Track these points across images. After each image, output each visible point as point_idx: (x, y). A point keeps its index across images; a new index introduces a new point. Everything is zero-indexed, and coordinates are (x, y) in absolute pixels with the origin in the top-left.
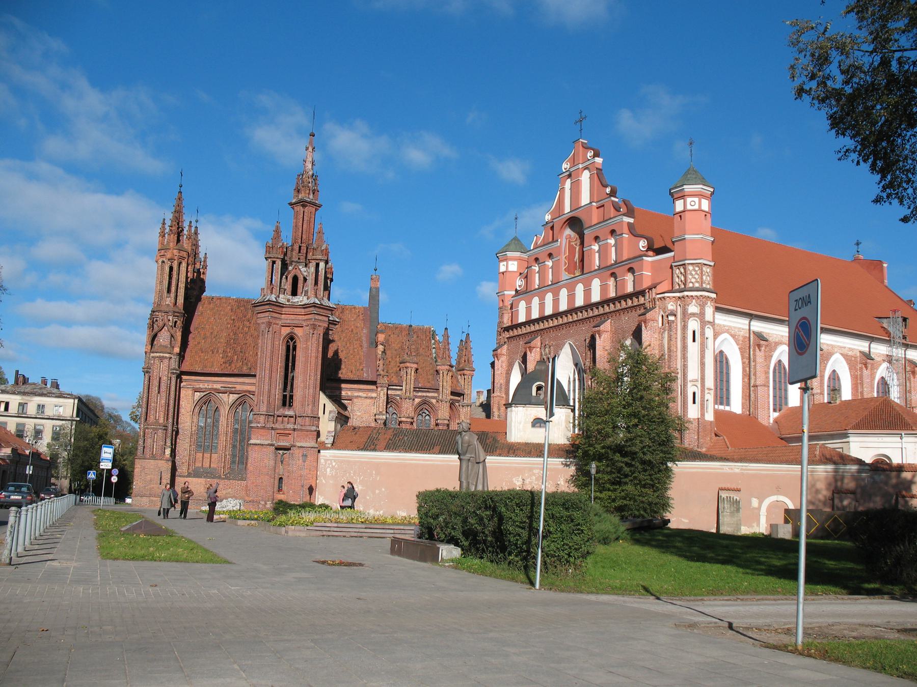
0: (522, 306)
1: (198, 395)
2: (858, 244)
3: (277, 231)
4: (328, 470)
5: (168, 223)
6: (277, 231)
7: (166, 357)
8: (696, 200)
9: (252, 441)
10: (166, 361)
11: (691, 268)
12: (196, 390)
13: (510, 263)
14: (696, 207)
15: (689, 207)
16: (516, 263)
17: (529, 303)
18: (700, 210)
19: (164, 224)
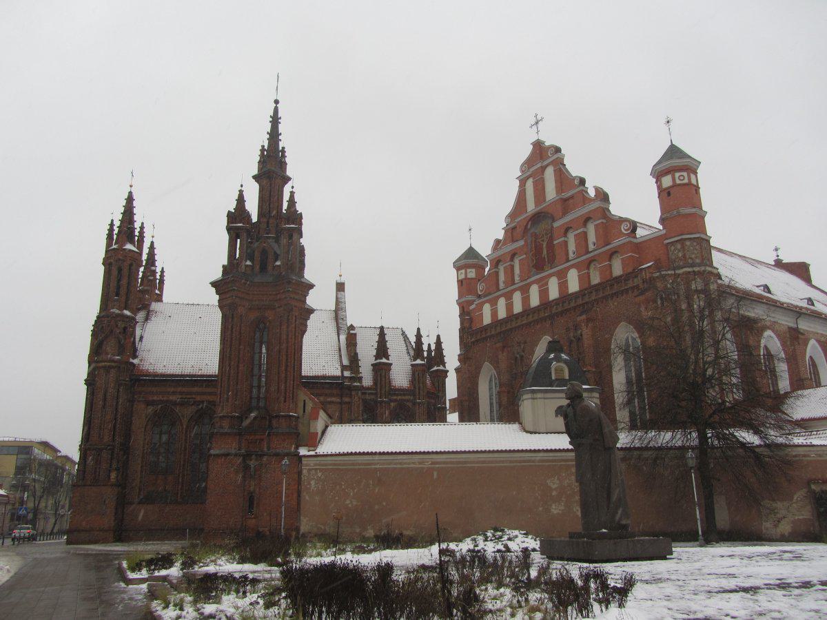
0: (487, 309)
1: (150, 409)
2: (776, 250)
3: (241, 200)
4: (313, 483)
5: (117, 223)
6: (241, 200)
7: (113, 367)
8: (685, 174)
9: (212, 452)
10: (113, 373)
11: (688, 243)
12: (148, 403)
13: (469, 270)
14: (686, 181)
15: (678, 182)
16: (474, 270)
17: (494, 303)
18: (690, 184)
19: (112, 225)
